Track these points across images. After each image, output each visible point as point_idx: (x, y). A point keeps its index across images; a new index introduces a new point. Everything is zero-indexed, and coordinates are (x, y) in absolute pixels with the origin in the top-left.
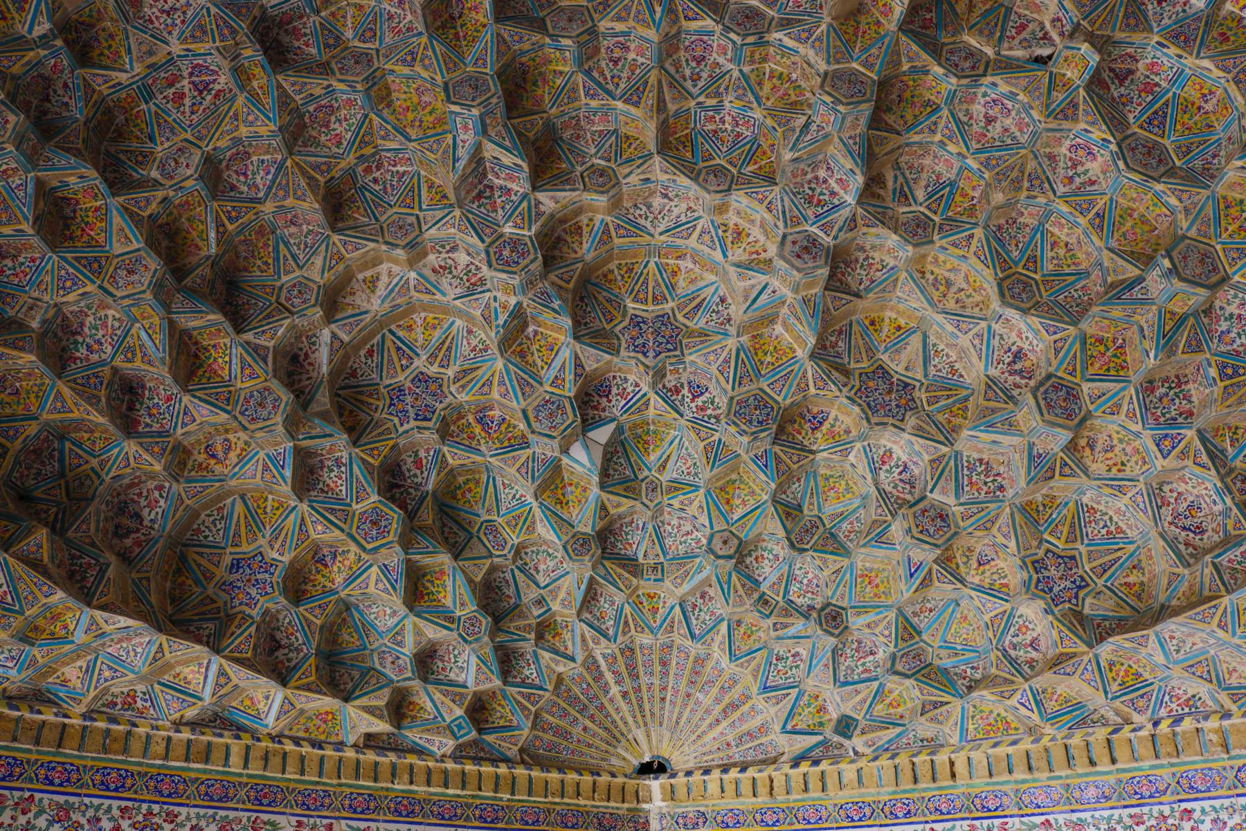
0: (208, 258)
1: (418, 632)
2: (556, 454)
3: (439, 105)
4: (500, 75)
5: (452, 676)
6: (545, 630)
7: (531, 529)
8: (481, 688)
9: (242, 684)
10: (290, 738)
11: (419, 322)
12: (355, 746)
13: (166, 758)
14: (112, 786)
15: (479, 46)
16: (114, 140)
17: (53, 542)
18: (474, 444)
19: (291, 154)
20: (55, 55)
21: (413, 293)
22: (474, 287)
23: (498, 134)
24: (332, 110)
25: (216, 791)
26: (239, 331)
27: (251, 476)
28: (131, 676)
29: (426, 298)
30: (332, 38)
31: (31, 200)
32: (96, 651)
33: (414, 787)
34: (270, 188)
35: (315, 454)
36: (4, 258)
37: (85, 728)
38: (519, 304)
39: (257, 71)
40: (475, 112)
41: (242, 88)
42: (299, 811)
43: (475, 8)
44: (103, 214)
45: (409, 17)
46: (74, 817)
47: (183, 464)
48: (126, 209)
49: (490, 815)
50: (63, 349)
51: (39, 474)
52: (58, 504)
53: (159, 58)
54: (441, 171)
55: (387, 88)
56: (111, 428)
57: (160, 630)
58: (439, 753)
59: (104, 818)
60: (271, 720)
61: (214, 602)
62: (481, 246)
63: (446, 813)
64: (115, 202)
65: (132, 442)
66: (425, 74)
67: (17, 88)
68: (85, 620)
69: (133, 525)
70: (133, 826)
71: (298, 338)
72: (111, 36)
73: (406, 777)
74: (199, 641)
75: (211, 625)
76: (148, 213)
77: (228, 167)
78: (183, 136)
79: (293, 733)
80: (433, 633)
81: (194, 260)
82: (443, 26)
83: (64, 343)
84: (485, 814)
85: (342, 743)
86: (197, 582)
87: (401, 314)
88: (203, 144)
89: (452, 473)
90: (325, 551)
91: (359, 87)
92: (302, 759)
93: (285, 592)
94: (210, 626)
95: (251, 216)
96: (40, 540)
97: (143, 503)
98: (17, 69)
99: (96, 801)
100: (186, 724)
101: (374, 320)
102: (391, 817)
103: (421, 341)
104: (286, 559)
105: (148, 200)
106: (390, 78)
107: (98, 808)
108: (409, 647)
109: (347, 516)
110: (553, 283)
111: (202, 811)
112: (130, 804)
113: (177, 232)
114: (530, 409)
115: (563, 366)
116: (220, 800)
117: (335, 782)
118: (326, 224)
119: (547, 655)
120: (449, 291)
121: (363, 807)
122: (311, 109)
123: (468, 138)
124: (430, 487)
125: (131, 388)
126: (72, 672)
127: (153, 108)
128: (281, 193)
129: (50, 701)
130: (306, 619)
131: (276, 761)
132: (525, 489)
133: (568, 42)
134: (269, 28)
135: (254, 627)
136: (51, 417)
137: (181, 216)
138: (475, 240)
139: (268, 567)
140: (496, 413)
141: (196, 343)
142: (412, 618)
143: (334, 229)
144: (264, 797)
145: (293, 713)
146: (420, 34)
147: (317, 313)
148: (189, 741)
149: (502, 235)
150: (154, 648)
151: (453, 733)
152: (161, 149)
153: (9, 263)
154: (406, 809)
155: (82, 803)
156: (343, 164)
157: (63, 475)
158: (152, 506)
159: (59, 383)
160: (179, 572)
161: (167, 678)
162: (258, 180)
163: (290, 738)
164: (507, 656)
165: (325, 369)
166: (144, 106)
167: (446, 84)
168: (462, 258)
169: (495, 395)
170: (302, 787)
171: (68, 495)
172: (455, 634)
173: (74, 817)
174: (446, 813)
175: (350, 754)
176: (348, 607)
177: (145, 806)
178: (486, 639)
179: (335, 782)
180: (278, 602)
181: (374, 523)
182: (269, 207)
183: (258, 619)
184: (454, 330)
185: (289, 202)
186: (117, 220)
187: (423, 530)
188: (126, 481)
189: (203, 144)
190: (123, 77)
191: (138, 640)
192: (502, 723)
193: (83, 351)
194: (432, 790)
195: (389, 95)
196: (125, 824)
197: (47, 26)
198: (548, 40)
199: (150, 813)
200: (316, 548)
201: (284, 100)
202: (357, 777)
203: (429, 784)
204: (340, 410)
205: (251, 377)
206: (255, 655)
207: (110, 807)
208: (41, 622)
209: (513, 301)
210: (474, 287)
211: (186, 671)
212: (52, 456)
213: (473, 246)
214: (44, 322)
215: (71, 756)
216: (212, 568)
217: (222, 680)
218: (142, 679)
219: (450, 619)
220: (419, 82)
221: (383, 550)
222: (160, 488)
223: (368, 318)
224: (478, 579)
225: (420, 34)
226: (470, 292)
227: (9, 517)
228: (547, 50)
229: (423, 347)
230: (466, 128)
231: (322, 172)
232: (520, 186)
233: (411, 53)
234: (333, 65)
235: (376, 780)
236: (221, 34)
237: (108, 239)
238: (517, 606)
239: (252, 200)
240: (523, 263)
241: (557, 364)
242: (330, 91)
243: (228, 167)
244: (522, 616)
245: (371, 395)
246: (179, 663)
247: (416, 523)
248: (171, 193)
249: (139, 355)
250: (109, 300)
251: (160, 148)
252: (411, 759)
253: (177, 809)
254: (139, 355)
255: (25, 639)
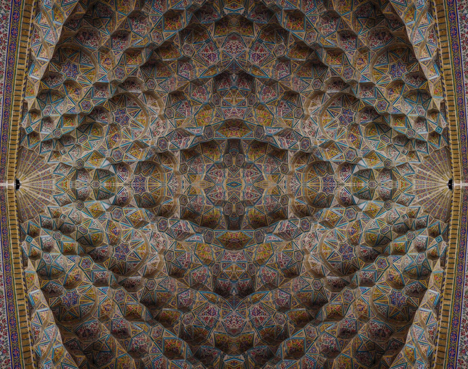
0: (306, 310)
1: (412, 251)
2: (362, 212)
3: (263, 245)
4: (255, 228)
5: (424, 242)
6: (411, 216)
7: (383, 219)
8: (428, 233)
9: (427, 301)
10: (442, 287)
11: (325, 251)
12: (444, 269)
13: (447, 322)
14: (455, 337)
15: (247, 234)
16: (273, 337)
17: (387, 354)
18: (359, 236)
19: (277, 287)
20: (249, 354)
21: (316, 253)
22: (315, 236)
23: (272, 229)
24: (265, 276)
25: (457, 308)
26: (327, 302)
27: (368, 299)
28: (424, 332)
29: (318, 249)
30: (245, 276)
31: (290, 361)
32: (417, 342)
33: (456, 253)
34: (287, 293)
35: (362, 280)
36: (307, 368)
37: (439, 345)
38: (320, 223)
39: (254, 297)
40: (265, 235)
41: (259, 301)
42: (462, 285)
43: (236, 235)
44: (294, 340)
45: (239, 254)
46: (464, 348)
47: (365, 318)
48: (293, 333)
49: (463, 231)
50: (332, 351)
51: (367, 358)
52: (376, 353)
53: (250, 324)
54: (282, 245)
55: (259, 260)
56: (355, 338)
57: (411, 324)
58: (446, 245)
59: (464, 340)
60: (437, 293)
61: (403, 309)
62: (303, 234)
63: (463, 243)
64: (291, 337)
65: (358, 332)
66: (255, 249)
67: (259, 364)
68: (409, 345)
69: (381, 332)
70: (466, 331)
71: (329, 285)
72: (244, 338)
73: (453, 255)
74: (415, 313)
75: (410, 310)
76: (294, 327)
77: (281, 305)
78: (272, 317)
79: (440, 287)
80: (412, 247)
81: (307, 314)
82: (241, 244)
83: (331, 351)
84: (463, 232)
85: (443, 273)
86: (398, 313)
87: (323, 257)
88: (275, 312)
89: (367, 242)
90: (389, 277)
91: (258, 268)
92: (448, 284)
93: (401, 289)
94: (410, 310)
95: (295, 298)
96: (386, 358)
97: (376, 329)
98: (253, 364)
99: (460, 342)
100: (438, 317)
101: (324, 264)
102: (464, 259)
103: (330, 251)
104: (391, 288)
105: (291, 327)
106: (256, 259)
107: (461, 341)
108: (416, 254)
109: (379, 271)
110: (314, 213)
111: (463, 312)
112: (460, 332)
113: (299, 319)
114: (349, 220)
115: (337, 210)
116: (459, 307)
117: (454, 275)
118: (297, 277)
119: (418, 215)
120: (316, 242)
121: (461, 267)
122: (265, 281)
123: (273, 237)
124: (371, 248)
125: (343, 332)
126: (423, 349)
127: (264, 326)
128: (288, 290)
129: (431, 355)
130: (408, 283)
131: (448, 291)
132: (372, 221)
133: (246, 209)
134: (242, 293)
135: (411, 298)
136: (351, 355)
137: (295, 318)
138: (302, 235)
139: (394, 294)
140: (350, 229)
141: (331, 314)
142: (408, 253)
143: (299, 275)
144: (458, 295)
145: (435, 286)
146: (243, 251)
147: (322, 280)
148: (443, 316)
149: (300, 228)
150: (417, 326)
151: (440, 242)
152: (276, 324)
153: (308, 367)
154: (462, 255)
155: (460, 346)
156: (280, 272)
157: (368, 351)
158: (377, 327)
159: (342, 352)
160: (395, 319)
161: (425, 322)
162: (285, 296)
163: (442, 287)
164: (419, 226)
165: (338, 278)
166: (264, 329)
167: (258, 243)
168: (307, 239)
169: (345, 230)
170: (456, 284)
171: (373, 350)
172: (412, 241)
173: (464, 348)
174: (463, 243)
175: (446, 271)
176: (405, 271)
177: (461, 328)
178: (414, 232)
179: (454, 275)
180: (404, 291)
181: (381, 264)
182: (292, 293)
183: (408, 296)
184: (327, 241)
185: (291, 288)
186: (296, 336)
187: (383, 250)
188: (369, 333)
189: (275, 312)
190: (256, 334)
191: (414, 330)
192: (437, 228)
193: (333, 346)
194: (456, 247)
195: (261, 260)
196: (466, 334)
197: (241, 356)
198: (245, 215)
199: (463, 327)
200: (389, 280)
201: (262, 289)
202: (453, 268)
203: (455, 248)
204: (349, 273)
205: (340, 298)
206: (418, 297)
207: (461, 338)
208: (409, 358)
209: (319, 225)
210: (315, 236)
211: (423, 317)
212: (362, 354)
213: (303, 236)
214: (325, 357)
215: (447, 349)
216: (394, 309)
217: (426, 306)
218: (425, 329)
219: (408, 243)
220: (257, 251)
221: (389, 261)
222: (371, 324)
223: (323, 265)
224: (397, 234)
225: (243, 251)
226: (316, 237)
227: (380, 366)
228: (248, 215)
229: (332, 250)
230: (270, 238)
231: (283, 278)
232: (286, 223)
233: (249, 253)
234: (252, 275)
235: (454, 263)
236: (244, 307)
237: (301, 338)
238: (405, 224)
239: (290, 298)
240: (308, 222)
241: (336, 212)
242: (260, 276)
243: (281, 305)
244: (407, 222)
245: (345, 265)
246: (421, 319)
247: (381, 252)
248: (288, 321)
249: (334, 330)
250: (319, 338)
251: (276, 324)
252: (448, 253)
253: (462, 319)
254: (334, 330)
255: (414, 362)
